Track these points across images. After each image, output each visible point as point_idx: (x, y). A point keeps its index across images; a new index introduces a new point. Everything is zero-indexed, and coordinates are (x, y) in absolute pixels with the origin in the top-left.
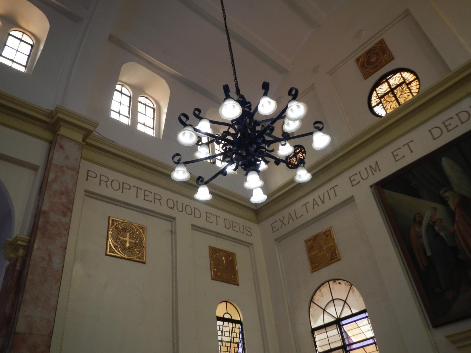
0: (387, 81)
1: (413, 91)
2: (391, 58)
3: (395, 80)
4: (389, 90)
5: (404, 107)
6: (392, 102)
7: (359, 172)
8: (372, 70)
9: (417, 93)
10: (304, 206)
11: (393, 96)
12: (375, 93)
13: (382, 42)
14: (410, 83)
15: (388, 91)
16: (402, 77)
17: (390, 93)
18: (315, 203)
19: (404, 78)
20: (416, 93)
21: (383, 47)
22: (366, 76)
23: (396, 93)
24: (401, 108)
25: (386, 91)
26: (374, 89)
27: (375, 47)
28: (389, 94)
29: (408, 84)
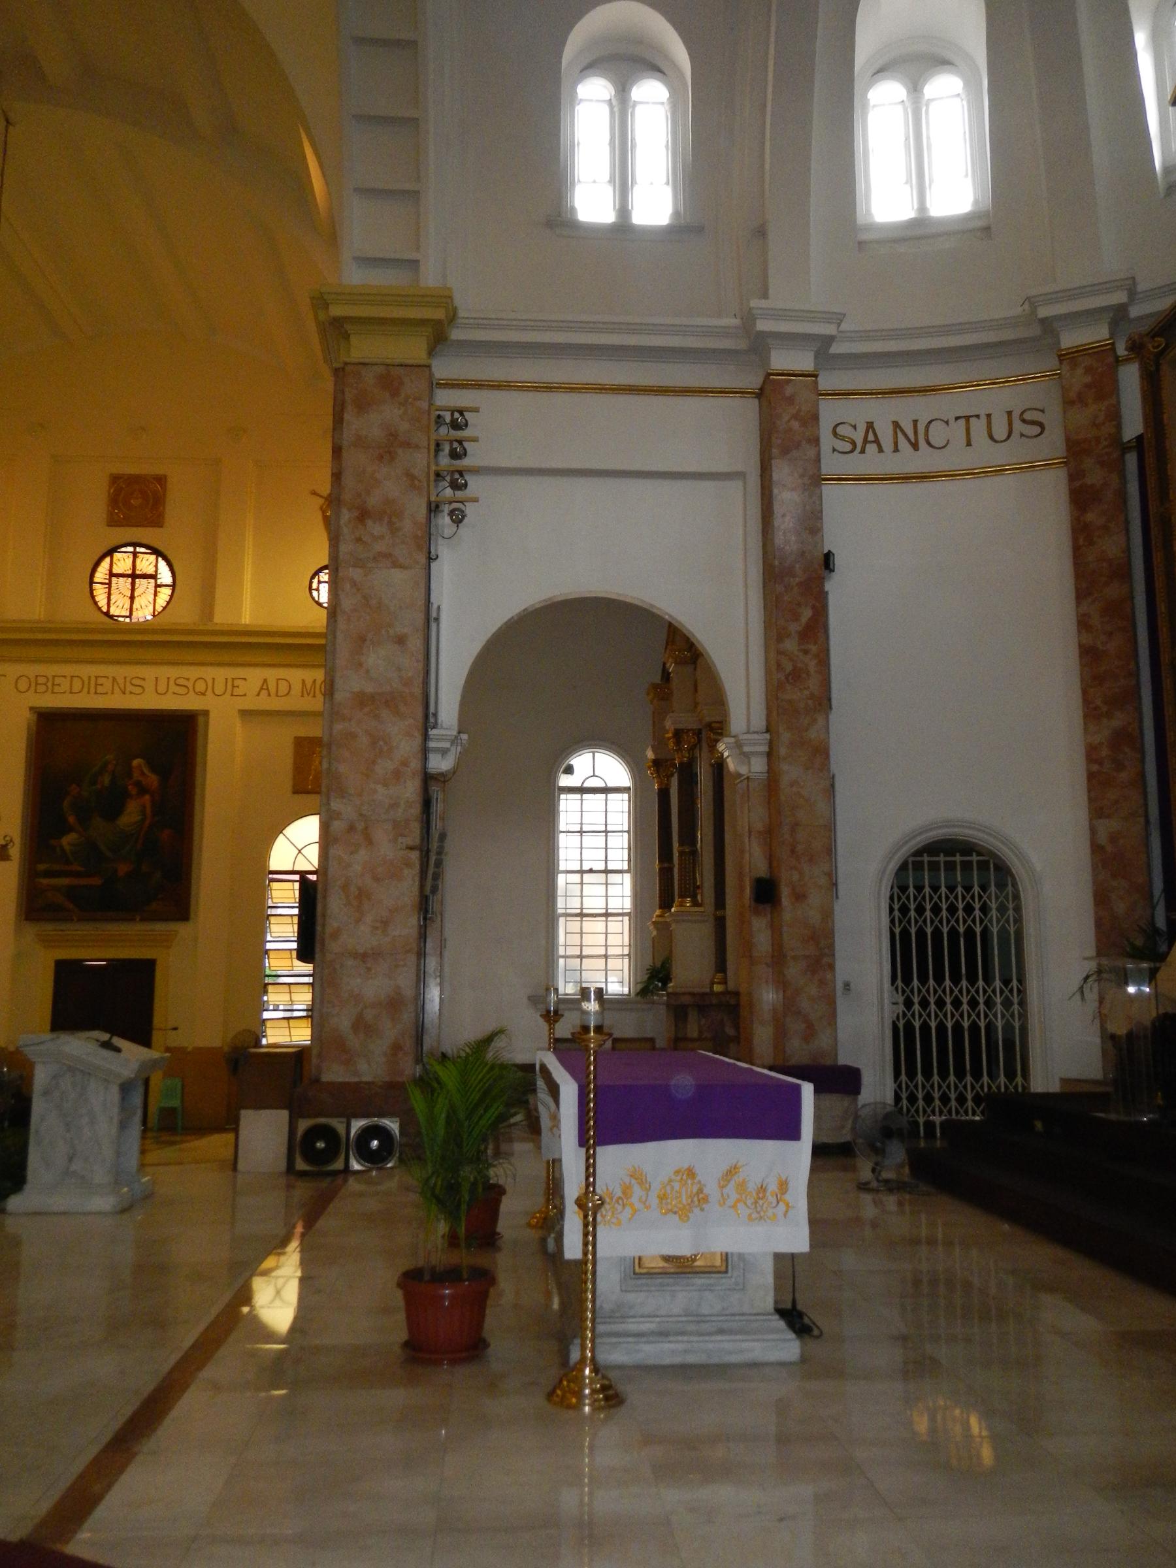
2: (156, 521)
4: (130, 572)
12: (108, 560)
13: (161, 480)
14: (160, 586)
16: (156, 566)
22: (113, 522)
26: (110, 553)
29: (157, 586)
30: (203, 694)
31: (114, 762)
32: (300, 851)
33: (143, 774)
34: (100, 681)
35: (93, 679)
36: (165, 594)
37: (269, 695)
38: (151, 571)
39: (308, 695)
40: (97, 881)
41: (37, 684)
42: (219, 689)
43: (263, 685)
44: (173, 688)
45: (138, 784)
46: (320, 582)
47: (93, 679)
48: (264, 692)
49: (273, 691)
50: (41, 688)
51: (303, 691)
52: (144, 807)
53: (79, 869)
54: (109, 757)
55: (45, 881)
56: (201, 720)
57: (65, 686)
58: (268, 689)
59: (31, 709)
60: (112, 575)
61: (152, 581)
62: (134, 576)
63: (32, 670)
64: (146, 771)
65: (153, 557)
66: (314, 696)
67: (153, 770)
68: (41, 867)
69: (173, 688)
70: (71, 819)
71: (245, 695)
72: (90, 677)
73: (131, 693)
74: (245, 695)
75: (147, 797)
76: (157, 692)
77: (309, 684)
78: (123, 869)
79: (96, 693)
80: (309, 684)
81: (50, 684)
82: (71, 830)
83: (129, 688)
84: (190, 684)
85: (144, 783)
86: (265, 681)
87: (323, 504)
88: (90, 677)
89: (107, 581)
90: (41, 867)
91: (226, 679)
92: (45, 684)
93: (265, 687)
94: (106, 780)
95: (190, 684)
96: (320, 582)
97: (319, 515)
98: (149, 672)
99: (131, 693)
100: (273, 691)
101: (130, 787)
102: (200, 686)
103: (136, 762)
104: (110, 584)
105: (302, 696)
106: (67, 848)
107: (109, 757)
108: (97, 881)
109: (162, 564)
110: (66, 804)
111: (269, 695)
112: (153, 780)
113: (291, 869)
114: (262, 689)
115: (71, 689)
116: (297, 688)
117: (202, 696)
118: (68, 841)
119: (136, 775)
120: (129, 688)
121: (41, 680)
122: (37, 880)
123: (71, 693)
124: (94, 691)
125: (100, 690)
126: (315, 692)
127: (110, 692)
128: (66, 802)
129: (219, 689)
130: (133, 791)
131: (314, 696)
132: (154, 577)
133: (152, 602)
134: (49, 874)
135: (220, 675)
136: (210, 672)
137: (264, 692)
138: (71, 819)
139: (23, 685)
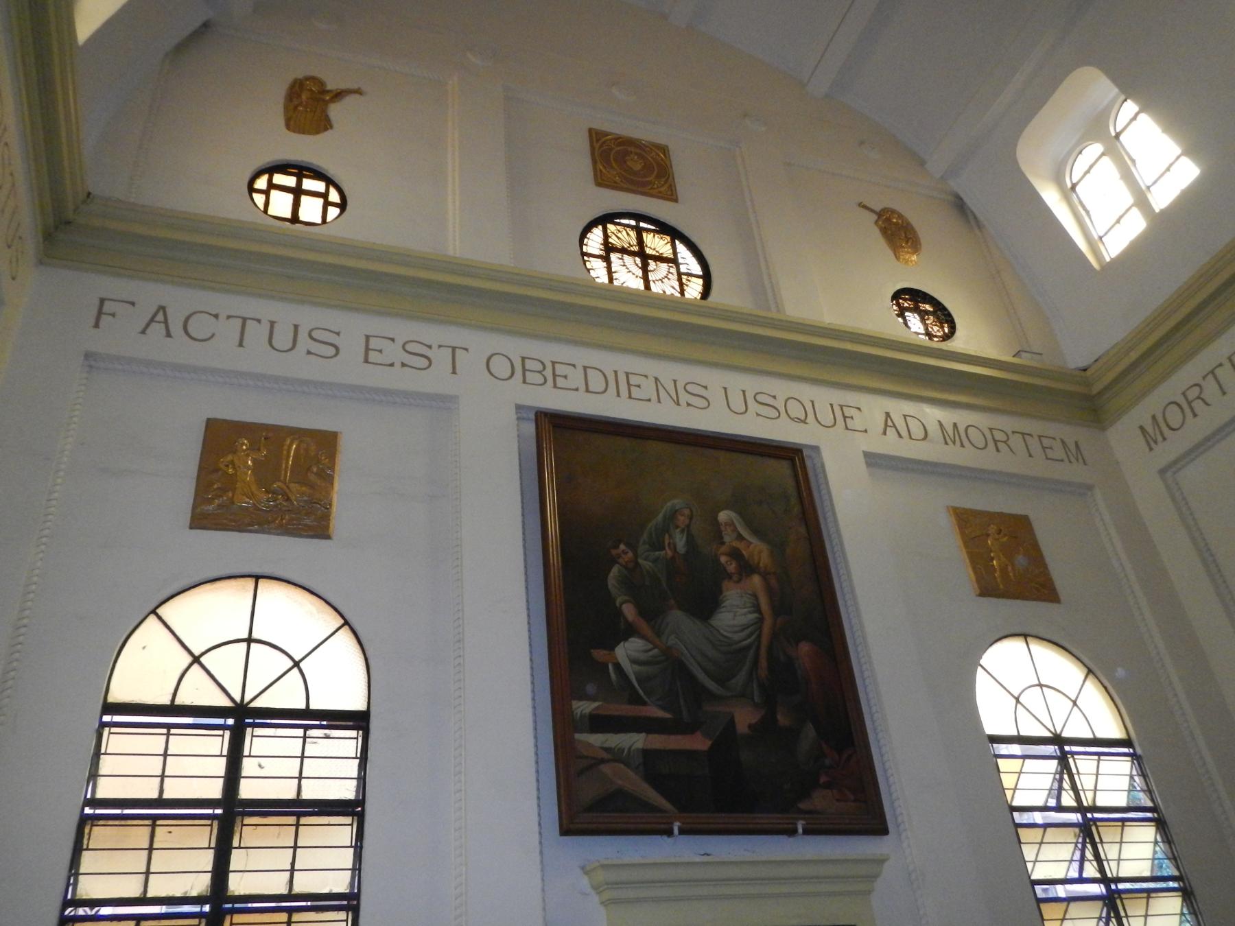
26: (604, 220)
31: (687, 512)
33: (740, 537)
34: (634, 379)
35: (622, 378)
40: (698, 743)
41: (524, 370)
45: (735, 554)
47: (622, 378)
48: (891, 431)
52: (755, 596)
53: (661, 714)
58: (894, 426)
63: (516, 347)
64: (745, 534)
68: (583, 708)
70: (629, 611)
72: (616, 372)
74: (866, 431)
75: (756, 580)
78: (745, 718)
82: (630, 631)
83: (684, 398)
84: (780, 404)
86: (888, 415)
88: (616, 372)
90: (583, 708)
92: (540, 372)
94: (680, 541)
98: (714, 379)
100: (904, 433)
101: (723, 559)
107: (677, 502)
108: (698, 743)
112: (758, 550)
114: (886, 425)
117: (802, 424)
118: (627, 652)
120: (684, 398)
122: (577, 736)
123: (587, 391)
128: (611, 574)
134: (598, 723)
135: (824, 398)
136: (807, 392)
137: (891, 431)
138: (629, 611)
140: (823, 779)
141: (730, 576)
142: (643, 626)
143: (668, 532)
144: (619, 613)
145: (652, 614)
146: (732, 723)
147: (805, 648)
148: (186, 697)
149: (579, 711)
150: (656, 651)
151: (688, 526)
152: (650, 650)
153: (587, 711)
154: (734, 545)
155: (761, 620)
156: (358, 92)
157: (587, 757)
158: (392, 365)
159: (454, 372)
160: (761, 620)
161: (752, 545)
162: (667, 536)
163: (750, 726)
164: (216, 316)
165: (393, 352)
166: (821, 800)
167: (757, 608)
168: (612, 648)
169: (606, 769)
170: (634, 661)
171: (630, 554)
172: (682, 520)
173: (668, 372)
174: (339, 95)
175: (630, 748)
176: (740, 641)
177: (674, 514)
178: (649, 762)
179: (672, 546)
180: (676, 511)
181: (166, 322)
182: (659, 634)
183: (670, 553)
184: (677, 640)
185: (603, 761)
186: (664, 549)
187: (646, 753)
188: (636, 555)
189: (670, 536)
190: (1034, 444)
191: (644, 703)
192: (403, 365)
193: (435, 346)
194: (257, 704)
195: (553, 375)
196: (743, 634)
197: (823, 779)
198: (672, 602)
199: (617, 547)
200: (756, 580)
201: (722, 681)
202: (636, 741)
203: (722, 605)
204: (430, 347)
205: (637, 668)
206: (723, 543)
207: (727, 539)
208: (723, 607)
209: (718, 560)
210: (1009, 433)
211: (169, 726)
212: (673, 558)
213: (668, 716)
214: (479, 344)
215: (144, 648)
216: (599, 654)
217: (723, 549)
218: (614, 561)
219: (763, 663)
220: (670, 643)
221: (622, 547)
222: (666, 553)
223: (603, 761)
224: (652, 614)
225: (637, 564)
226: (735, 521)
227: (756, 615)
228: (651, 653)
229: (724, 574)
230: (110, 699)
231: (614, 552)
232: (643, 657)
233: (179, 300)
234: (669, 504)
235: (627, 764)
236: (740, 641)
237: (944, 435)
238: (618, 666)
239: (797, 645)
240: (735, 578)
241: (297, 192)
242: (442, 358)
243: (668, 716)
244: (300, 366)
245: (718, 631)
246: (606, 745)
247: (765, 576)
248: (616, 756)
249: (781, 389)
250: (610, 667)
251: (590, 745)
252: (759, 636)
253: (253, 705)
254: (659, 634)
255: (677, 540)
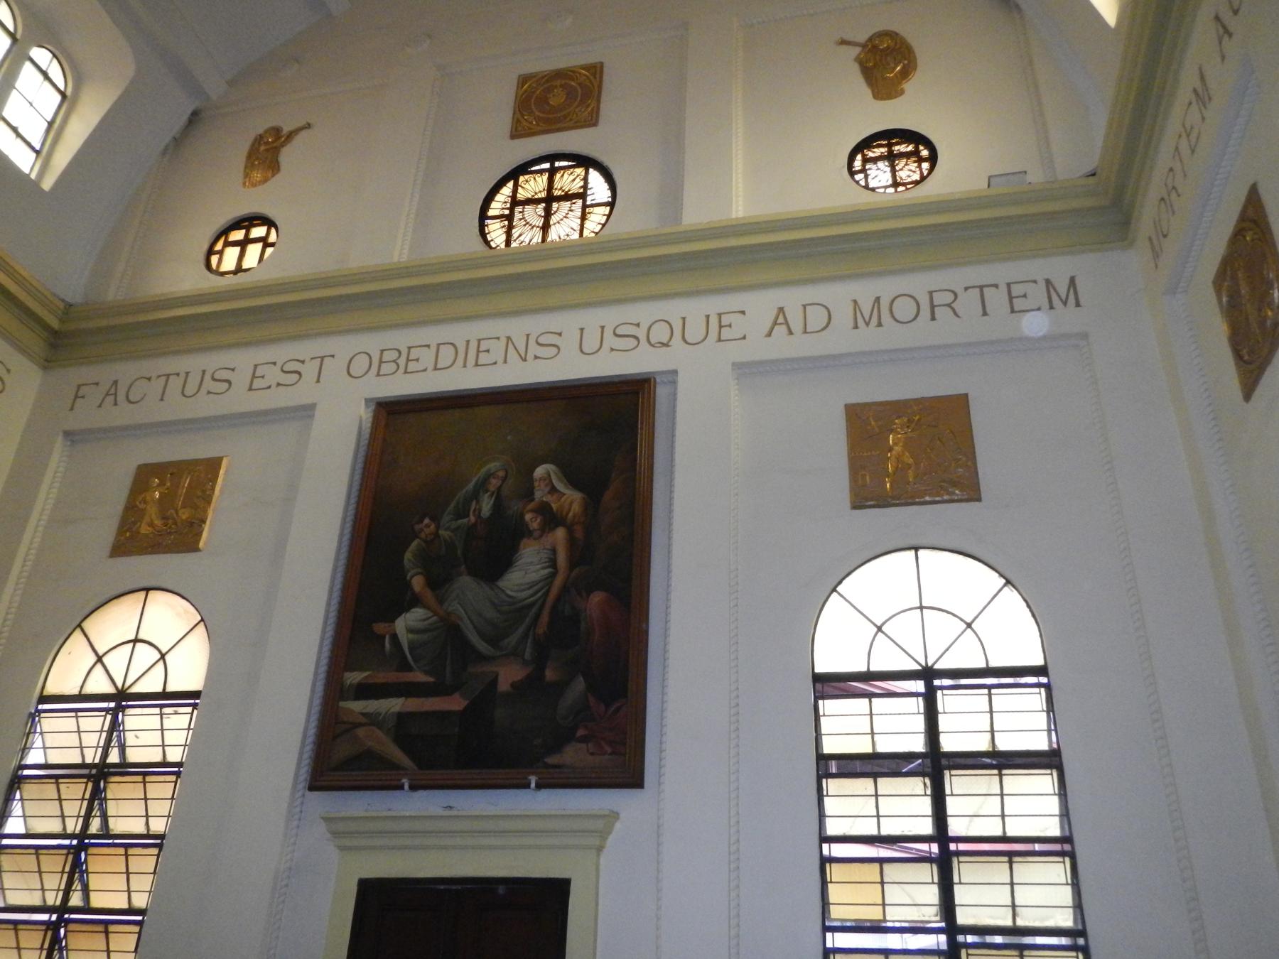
0: (552, 172)
1: (587, 224)
3: (568, 181)
4: (543, 195)
5: (513, 254)
6: (530, 227)
7: (187, 373)
8: (538, 125)
9: (593, 235)
10: (164, 378)
11: (543, 214)
12: (511, 184)
15: (540, 196)
17: (544, 205)
18: (113, 391)
19: (585, 187)
20: (593, 232)
21: (591, 81)
23: (553, 212)
24: (507, 255)
25: (536, 197)
26: (515, 174)
27: (573, 72)
28: (539, 206)
29: (585, 207)
30: (666, 345)
31: (501, 474)
32: (879, 629)
33: (553, 490)
35: (473, 345)
36: (597, 217)
37: (791, 333)
38: (576, 187)
39: (867, 324)
40: (455, 703)
42: (695, 332)
43: (777, 318)
44: (610, 340)
45: (544, 509)
46: (866, 160)
47: (473, 345)
48: (780, 330)
49: (797, 326)
50: (386, 368)
51: (856, 319)
52: (554, 551)
54: (493, 466)
55: (357, 706)
56: (661, 392)
57: (427, 357)
59: (367, 401)
60: (515, 202)
61: (580, 202)
62: (550, 199)
63: (372, 343)
64: (560, 486)
65: (580, 171)
66: (880, 324)
67: (574, 483)
68: (353, 678)
69: (610, 340)
70: (418, 583)
71: (744, 338)
72: (468, 342)
73: (536, 357)
75: (560, 533)
76: (582, 351)
77: (866, 308)
78: (509, 675)
79: (477, 365)
80: (866, 308)
81: (402, 361)
82: (416, 601)
83: (534, 349)
84: (641, 334)
85: (554, 506)
86: (781, 310)
87: (860, 54)
88: (468, 342)
89: (507, 212)
90: (353, 678)
91: (708, 317)
92: (394, 361)
93: (781, 320)
94: (486, 505)
95: (641, 334)
96: (866, 160)
97: (856, 68)
98: (568, 322)
99: (536, 357)
101: (528, 517)
102: (660, 333)
103: (539, 471)
104: (510, 218)
105: (856, 327)
106: (404, 638)
107: (493, 466)
108: (455, 703)
109: (595, 178)
110: (408, 556)
111: (791, 333)
112: (571, 500)
113: (863, 669)
114: (775, 323)
115: (436, 364)
116: (843, 315)
117: (665, 348)
118: (407, 624)
119: (540, 494)
121: (389, 356)
122: (342, 704)
124: (474, 363)
125: (484, 358)
126: (879, 317)
127: (501, 360)
129: (695, 332)
130: (532, 520)
131: (880, 324)
132: (582, 196)
133: (577, 228)
134: (365, 691)
135: (695, 310)
136: (674, 309)
137: (780, 330)
138: (418, 583)
139: (360, 364)
140: (580, 732)
141: (529, 533)
142: (429, 596)
143: (476, 499)
144: (408, 585)
145: (437, 583)
146: (494, 682)
147: (597, 597)
148: (91, 689)
149: (348, 682)
150: (435, 618)
151: (499, 489)
152: (430, 618)
153: (356, 681)
154: (544, 499)
155: (553, 575)
156: (308, 126)
157: (344, 723)
158: (269, 387)
159: (318, 381)
160: (553, 575)
161: (565, 497)
162: (474, 503)
163: (513, 685)
164: (149, 379)
165: (273, 375)
166: (572, 755)
167: (553, 563)
168: (393, 621)
169: (361, 732)
170: (410, 630)
171: (433, 527)
172: (494, 483)
173: (517, 328)
174: (291, 136)
175: (386, 713)
176: (526, 599)
177: (489, 475)
178: (402, 727)
179: (477, 513)
180: (492, 474)
181: (115, 394)
182: (441, 601)
183: (472, 519)
184: (458, 606)
185: (361, 725)
186: (468, 516)
187: (402, 717)
188: (438, 528)
189: (478, 502)
190: (996, 299)
191: (410, 669)
192: (279, 384)
193: (307, 360)
194: (135, 690)
195: (405, 361)
196: (531, 591)
197: (580, 732)
198: (463, 567)
199: (422, 521)
200: (560, 533)
201: (493, 641)
202: (394, 705)
203: (514, 565)
204: (303, 362)
205: (411, 636)
206: (533, 500)
207: (538, 495)
208: (516, 566)
209: (522, 516)
210: (960, 291)
211: (76, 710)
212: (475, 525)
213: (431, 679)
214: (342, 347)
215: (70, 653)
216: (380, 628)
217: (531, 506)
218: (416, 536)
219: (545, 618)
220: (450, 609)
221: (427, 521)
222: (469, 521)
223: (361, 725)
224: (437, 583)
225: (436, 535)
226: (553, 477)
227: (550, 570)
228: (430, 621)
229: (529, 533)
230: (45, 693)
231: (417, 527)
232: (420, 625)
233: (126, 371)
234: (484, 470)
235: (380, 728)
236: (526, 599)
237: (856, 319)
238: (394, 637)
239: (588, 596)
240: (536, 534)
241: (243, 244)
242: (310, 370)
243: (431, 679)
244: (205, 406)
245: (503, 591)
246: (364, 711)
247: (570, 531)
248: (372, 720)
249: (644, 313)
250: (387, 637)
251: (352, 712)
252: (548, 591)
253: (129, 691)
254: (441, 601)
255: (484, 505)
